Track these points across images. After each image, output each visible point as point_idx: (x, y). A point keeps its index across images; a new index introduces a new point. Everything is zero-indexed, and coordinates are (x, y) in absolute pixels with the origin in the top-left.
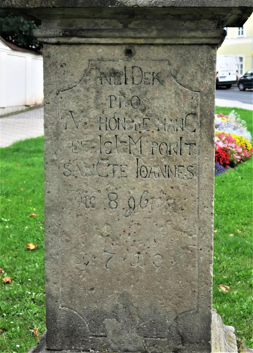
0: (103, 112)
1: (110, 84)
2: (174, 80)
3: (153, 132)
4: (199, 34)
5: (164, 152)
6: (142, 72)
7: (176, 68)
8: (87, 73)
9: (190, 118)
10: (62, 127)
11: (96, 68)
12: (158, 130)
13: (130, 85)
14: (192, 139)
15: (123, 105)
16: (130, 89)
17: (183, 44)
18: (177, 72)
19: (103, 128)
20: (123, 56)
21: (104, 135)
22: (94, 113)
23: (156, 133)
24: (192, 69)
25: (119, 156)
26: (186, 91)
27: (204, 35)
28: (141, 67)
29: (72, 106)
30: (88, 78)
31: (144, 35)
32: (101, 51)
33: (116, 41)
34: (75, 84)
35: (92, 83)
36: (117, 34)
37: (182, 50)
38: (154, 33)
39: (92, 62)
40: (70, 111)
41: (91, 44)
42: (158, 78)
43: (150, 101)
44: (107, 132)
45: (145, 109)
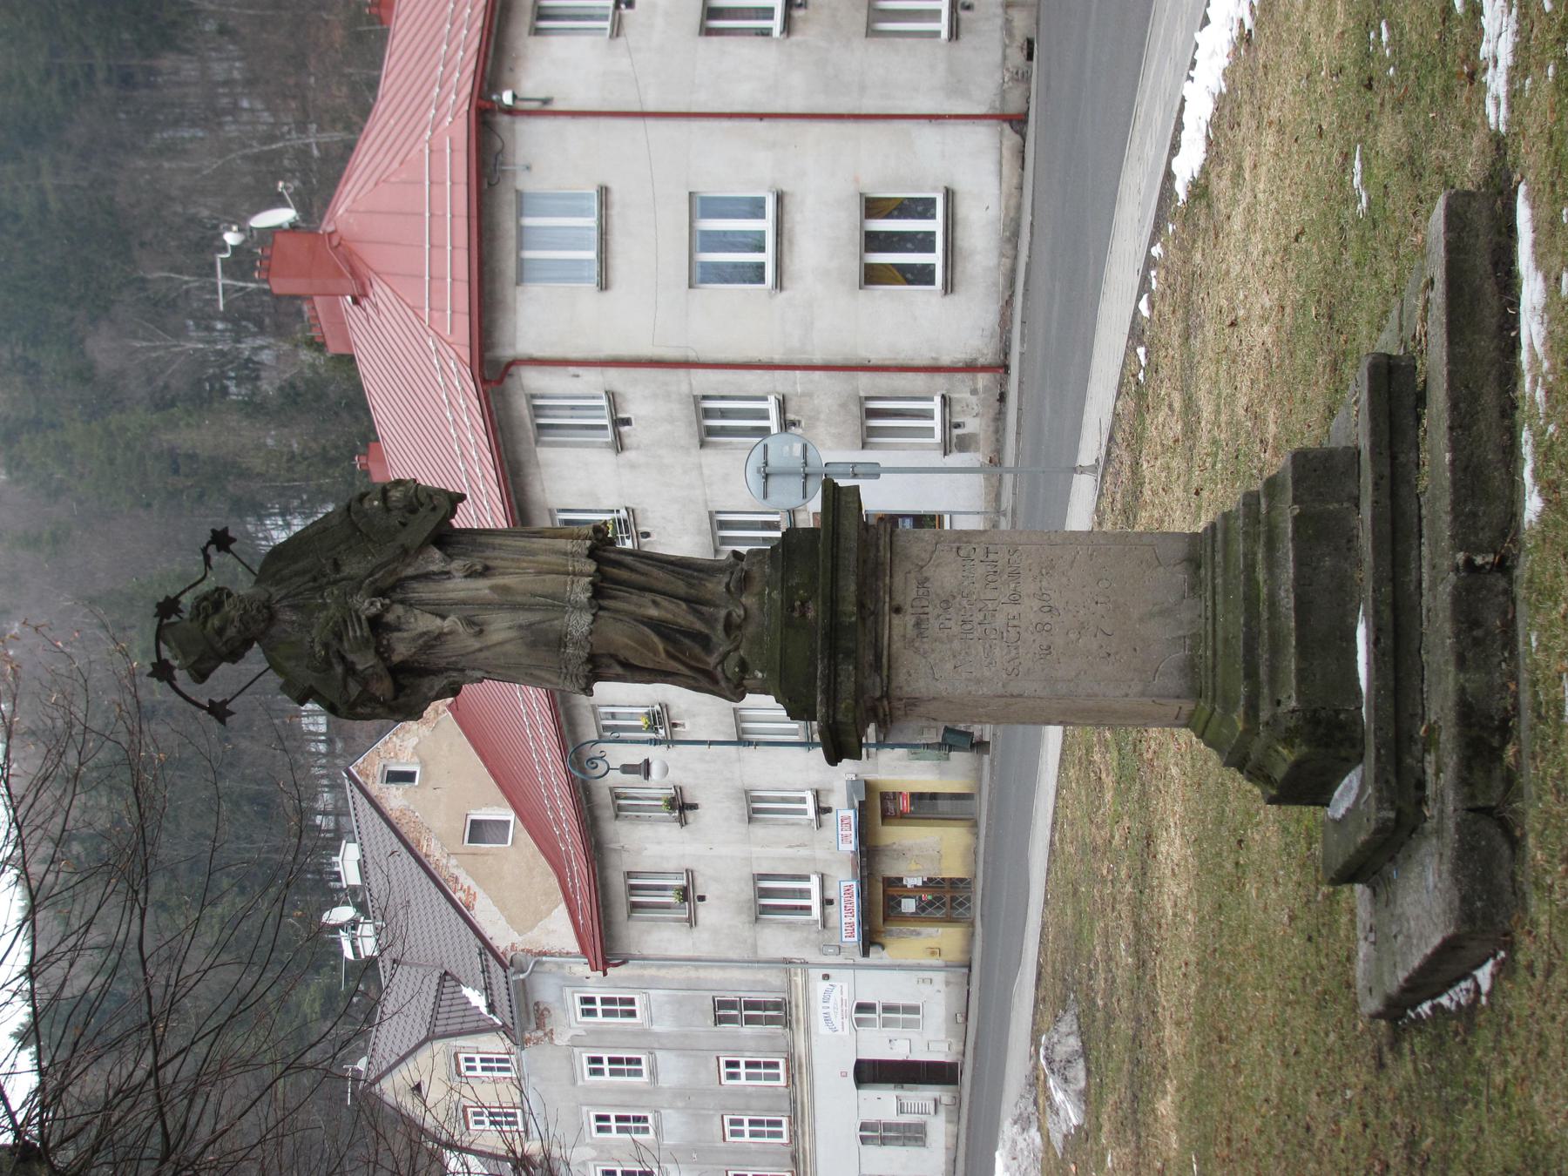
4: (882, 542)
5: (995, 578)
8: (917, 651)
9: (962, 553)
19: (970, 636)
22: (956, 645)
25: (1000, 620)
29: (949, 666)
35: (926, 646)
37: (896, 561)
41: (889, 645)
42: (923, 582)
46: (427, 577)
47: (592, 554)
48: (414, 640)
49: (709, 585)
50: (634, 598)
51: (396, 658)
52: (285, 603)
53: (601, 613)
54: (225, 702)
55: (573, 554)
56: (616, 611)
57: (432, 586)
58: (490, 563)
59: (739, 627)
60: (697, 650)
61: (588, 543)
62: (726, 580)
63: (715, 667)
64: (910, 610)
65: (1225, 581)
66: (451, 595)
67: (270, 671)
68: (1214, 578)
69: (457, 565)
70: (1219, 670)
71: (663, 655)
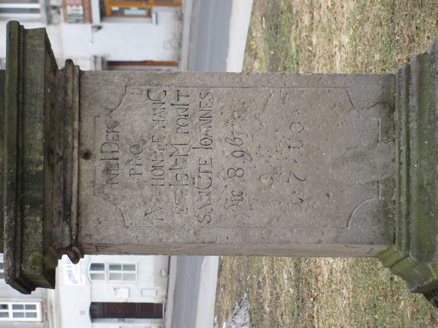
0: (145, 182)
1: (118, 175)
2: (115, 111)
3: (166, 133)
5: (186, 122)
6: (106, 143)
7: (103, 109)
8: (107, 197)
9: (152, 96)
10: (161, 223)
11: (102, 188)
12: (164, 127)
13: (121, 153)
14: (173, 94)
15: (139, 162)
16: (124, 154)
17: (79, 102)
18: (106, 108)
20: (90, 161)
21: (169, 181)
22: (147, 191)
23: (167, 129)
26: (126, 100)
27: (71, 80)
28: (101, 144)
29: (140, 213)
30: (112, 197)
31: (70, 139)
34: (118, 210)
36: (69, 165)
37: (85, 104)
39: (96, 192)
40: (145, 215)
41: (78, 192)
43: (135, 135)
44: (166, 178)
45: (143, 140)
64: (100, 155)
65: (420, 126)
68: (408, 122)
70: (413, 216)
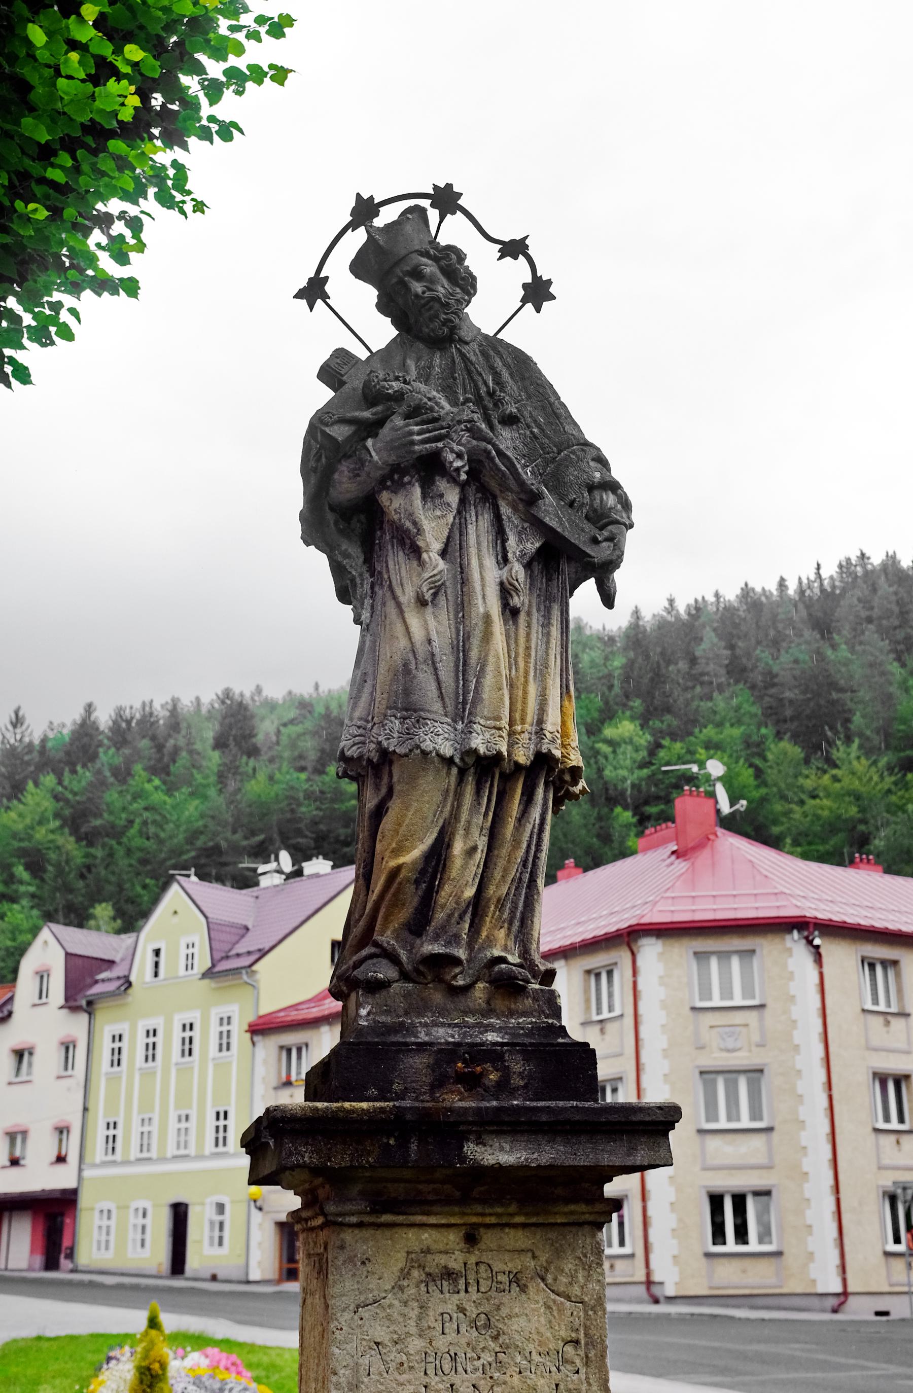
0: (431, 1343)
1: (442, 1292)
2: (542, 1285)
3: (511, 1376)
4: (582, 1207)
6: (492, 1271)
7: (545, 1264)
8: (405, 1274)
9: (569, 1349)
10: (363, 1372)
11: (419, 1266)
12: (520, 1372)
13: (475, 1296)
14: (575, 1387)
15: (463, 1329)
16: (474, 1302)
18: (547, 1270)
19: (431, 1372)
20: (462, 1245)
21: (433, 1384)
22: (416, 1344)
23: (516, 1377)
24: (569, 1265)
26: (562, 1303)
27: (590, 1209)
28: (491, 1262)
29: (381, 1333)
30: (405, 1283)
31: (499, 1210)
32: (426, 1236)
33: (453, 1220)
34: (384, 1295)
35: (413, 1291)
36: (456, 1209)
37: (552, 1235)
38: (513, 1208)
39: (413, 1256)
40: (375, 1343)
42: (517, 1280)
43: (506, 1321)
44: (437, 1379)
45: (498, 1335)
46: (500, 534)
47: (543, 760)
48: (411, 516)
49: (501, 934)
50: (478, 820)
51: (384, 497)
52: (458, 359)
53: (455, 771)
54: (325, 297)
55: (540, 732)
56: (459, 796)
57: (487, 539)
58: (522, 617)
59: (438, 979)
60: (404, 914)
61: (557, 753)
62: (514, 959)
63: (376, 944)
66: (474, 562)
67: (369, 354)
69: (518, 570)
71: (393, 863)
